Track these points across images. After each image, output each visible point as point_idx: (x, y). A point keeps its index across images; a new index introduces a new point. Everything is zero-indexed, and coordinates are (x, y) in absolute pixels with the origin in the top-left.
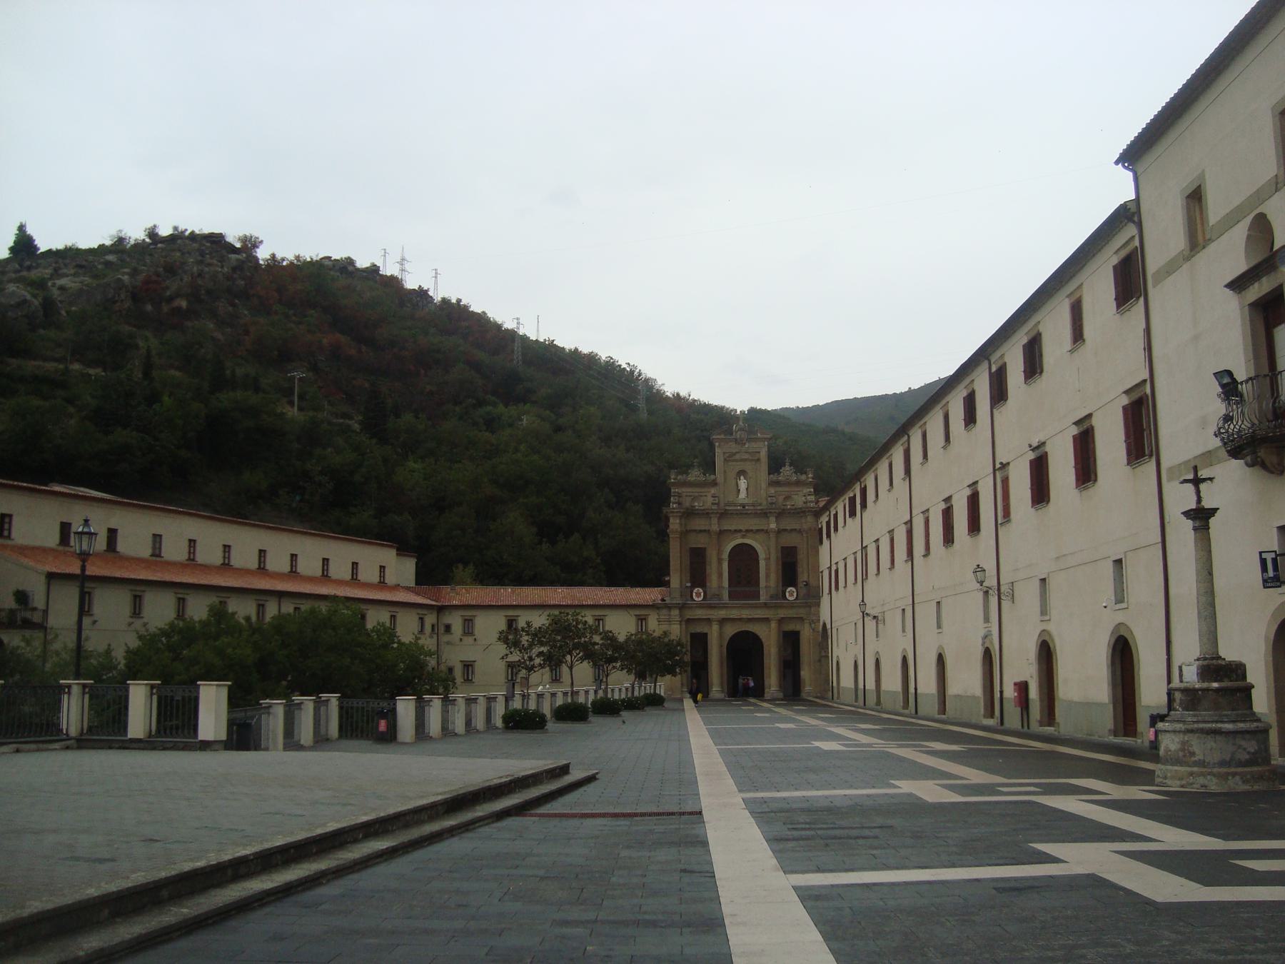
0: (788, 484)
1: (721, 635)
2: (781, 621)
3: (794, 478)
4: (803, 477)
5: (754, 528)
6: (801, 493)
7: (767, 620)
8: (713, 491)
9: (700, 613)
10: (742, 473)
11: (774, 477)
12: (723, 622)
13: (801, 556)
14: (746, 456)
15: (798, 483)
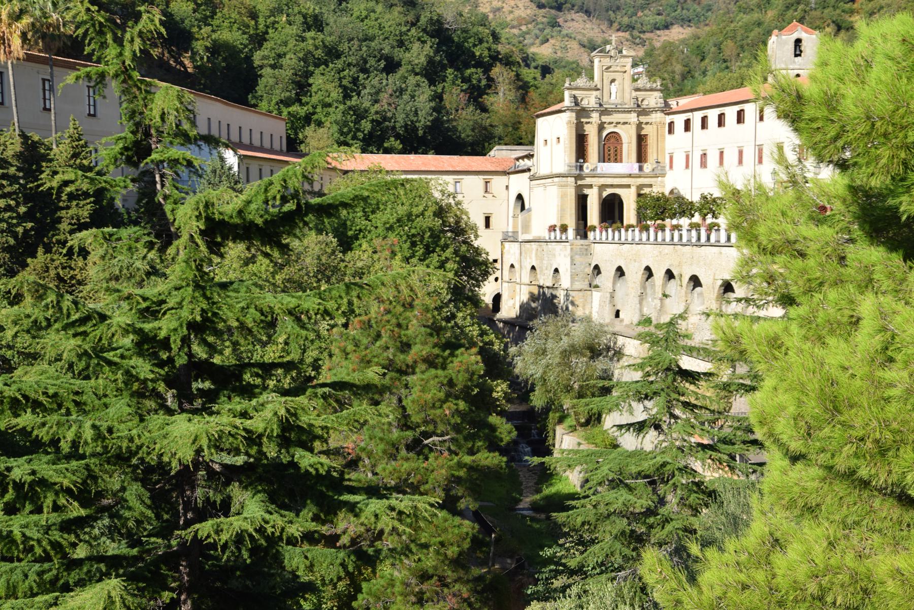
0: (646, 90)
1: (600, 195)
2: (640, 187)
3: (648, 86)
4: (654, 85)
5: (622, 121)
6: (653, 97)
7: (628, 186)
8: (595, 93)
9: (588, 181)
10: (613, 81)
11: (636, 85)
12: (602, 187)
13: (651, 142)
14: (618, 69)
15: (651, 90)
